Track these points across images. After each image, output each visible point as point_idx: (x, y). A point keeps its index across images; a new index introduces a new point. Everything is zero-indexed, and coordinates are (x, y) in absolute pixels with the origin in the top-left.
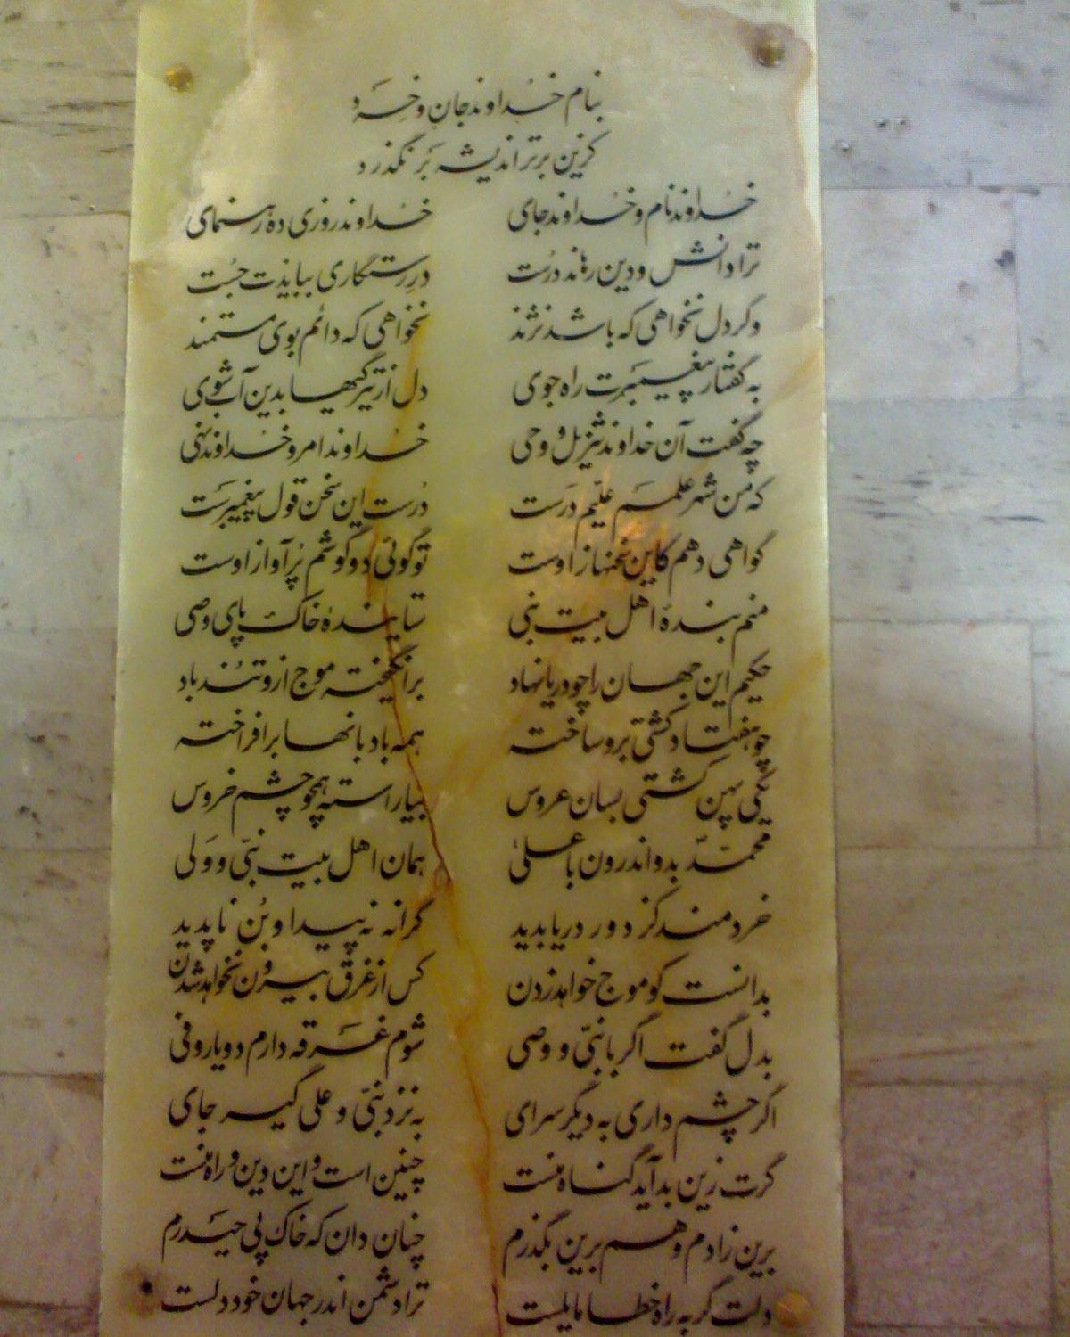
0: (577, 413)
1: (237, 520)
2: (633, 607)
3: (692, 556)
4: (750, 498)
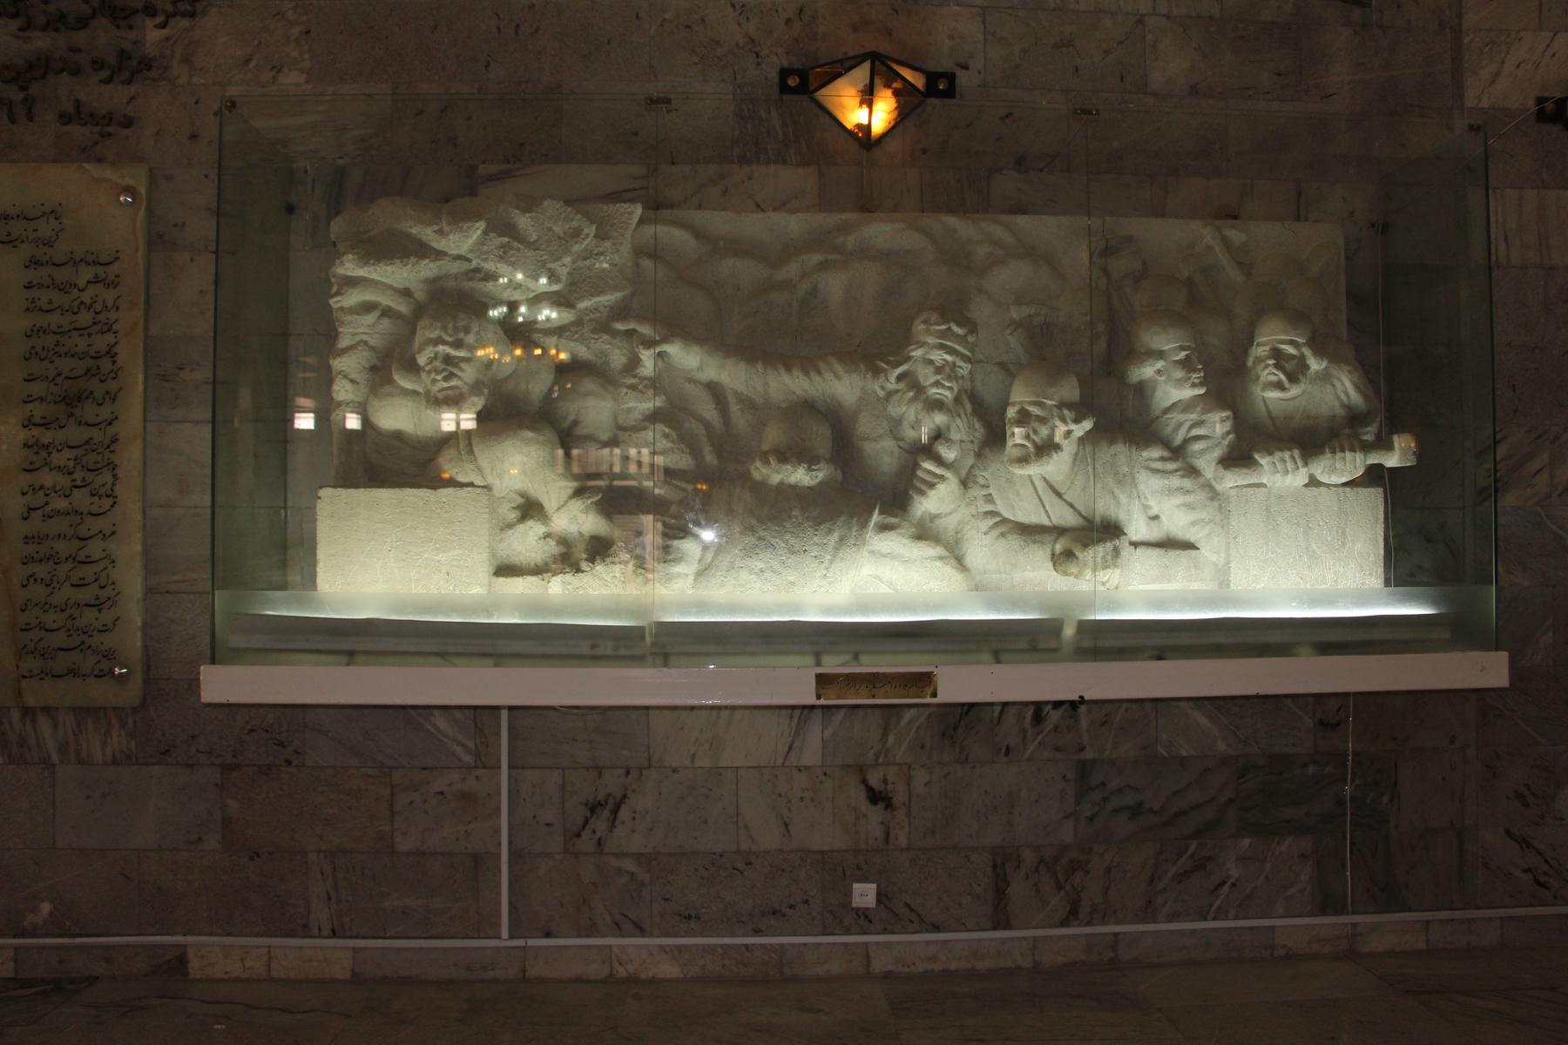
0: (50, 340)
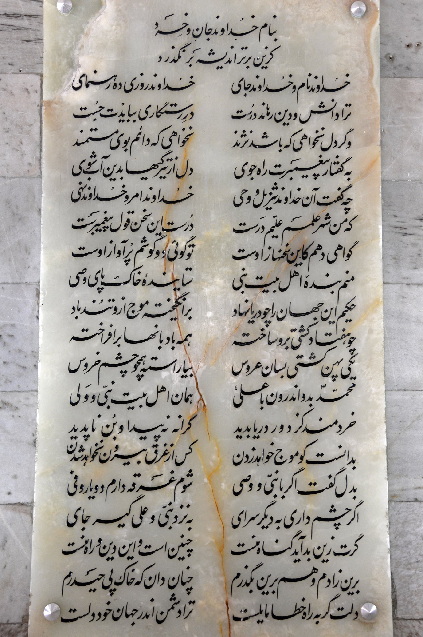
0: (265, 183)
1: (100, 230)
2: (291, 277)
3: (319, 252)
4: (346, 226)
